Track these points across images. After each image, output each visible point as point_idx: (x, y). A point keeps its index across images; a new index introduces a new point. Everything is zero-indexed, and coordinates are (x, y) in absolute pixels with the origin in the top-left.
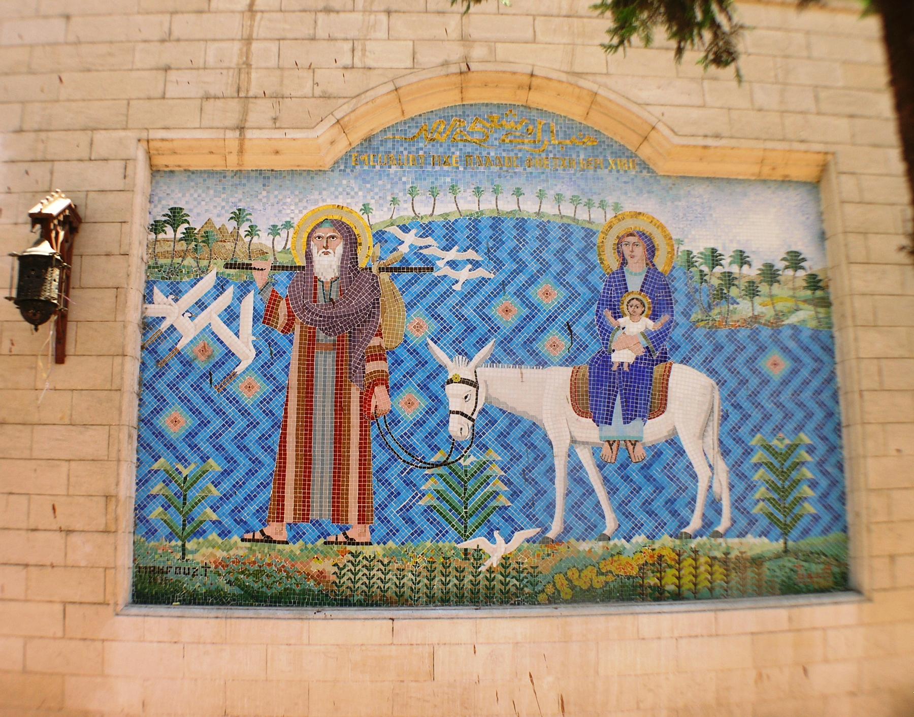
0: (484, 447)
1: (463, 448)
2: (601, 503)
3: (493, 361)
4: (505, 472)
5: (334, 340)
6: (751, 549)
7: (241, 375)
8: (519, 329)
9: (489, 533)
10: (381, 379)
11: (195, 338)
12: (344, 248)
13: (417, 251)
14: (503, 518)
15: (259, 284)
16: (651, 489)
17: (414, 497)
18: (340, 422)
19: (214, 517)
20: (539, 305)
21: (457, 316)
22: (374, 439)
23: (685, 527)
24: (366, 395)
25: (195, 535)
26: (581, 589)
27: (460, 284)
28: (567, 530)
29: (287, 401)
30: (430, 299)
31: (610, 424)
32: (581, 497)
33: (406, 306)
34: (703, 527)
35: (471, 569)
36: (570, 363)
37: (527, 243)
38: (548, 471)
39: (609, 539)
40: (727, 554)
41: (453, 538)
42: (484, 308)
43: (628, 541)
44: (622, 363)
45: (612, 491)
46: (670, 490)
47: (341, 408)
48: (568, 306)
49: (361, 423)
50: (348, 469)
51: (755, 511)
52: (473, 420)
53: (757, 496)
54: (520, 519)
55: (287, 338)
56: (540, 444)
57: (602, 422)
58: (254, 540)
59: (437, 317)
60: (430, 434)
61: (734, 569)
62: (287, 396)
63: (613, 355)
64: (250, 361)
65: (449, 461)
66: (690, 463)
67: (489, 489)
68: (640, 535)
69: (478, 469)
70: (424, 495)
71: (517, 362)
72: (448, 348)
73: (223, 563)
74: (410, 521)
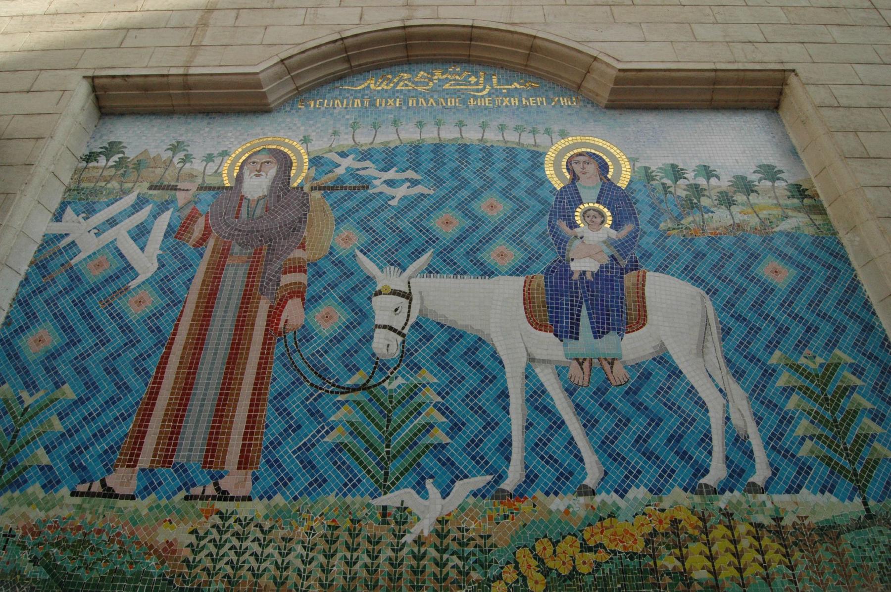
0: (416, 367)
1: (388, 368)
2: (577, 439)
3: (431, 271)
4: (443, 398)
5: (250, 253)
6: (814, 512)
7: (133, 289)
8: (461, 239)
9: (418, 483)
10: (297, 292)
11: (94, 253)
12: (278, 171)
13: (352, 173)
14: (440, 460)
15: (181, 201)
16: (643, 421)
17: (318, 432)
18: (240, 339)
19: (45, 460)
20: (483, 217)
21: (391, 228)
22: (278, 358)
23: (703, 475)
24: (277, 309)
25: (11, 486)
26: (559, 575)
27: (396, 200)
28: (530, 478)
29: (181, 316)
30: (363, 213)
31: (577, 339)
32: (547, 431)
33: (336, 220)
34: (730, 476)
35: (391, 539)
36: (521, 273)
37: (470, 164)
38: (499, 397)
39: (593, 493)
40: (778, 519)
41: (367, 490)
42: (421, 220)
43: (622, 496)
44: (584, 272)
45: (589, 424)
46: (671, 423)
47: (243, 325)
48: (516, 217)
49: (265, 339)
50: (238, 395)
51: (803, 452)
52: (404, 335)
53: (800, 432)
54: (463, 462)
55: (198, 252)
56: (488, 363)
57: (566, 337)
58: (89, 494)
59: (368, 229)
60: (348, 351)
61: (795, 544)
62: (182, 311)
63: (572, 264)
64: (149, 275)
65: (373, 382)
66: (692, 387)
67: (420, 420)
68: (638, 487)
69: (407, 394)
70: (332, 428)
71: (458, 272)
72: (378, 259)
73: (35, 530)
74: (309, 465)
